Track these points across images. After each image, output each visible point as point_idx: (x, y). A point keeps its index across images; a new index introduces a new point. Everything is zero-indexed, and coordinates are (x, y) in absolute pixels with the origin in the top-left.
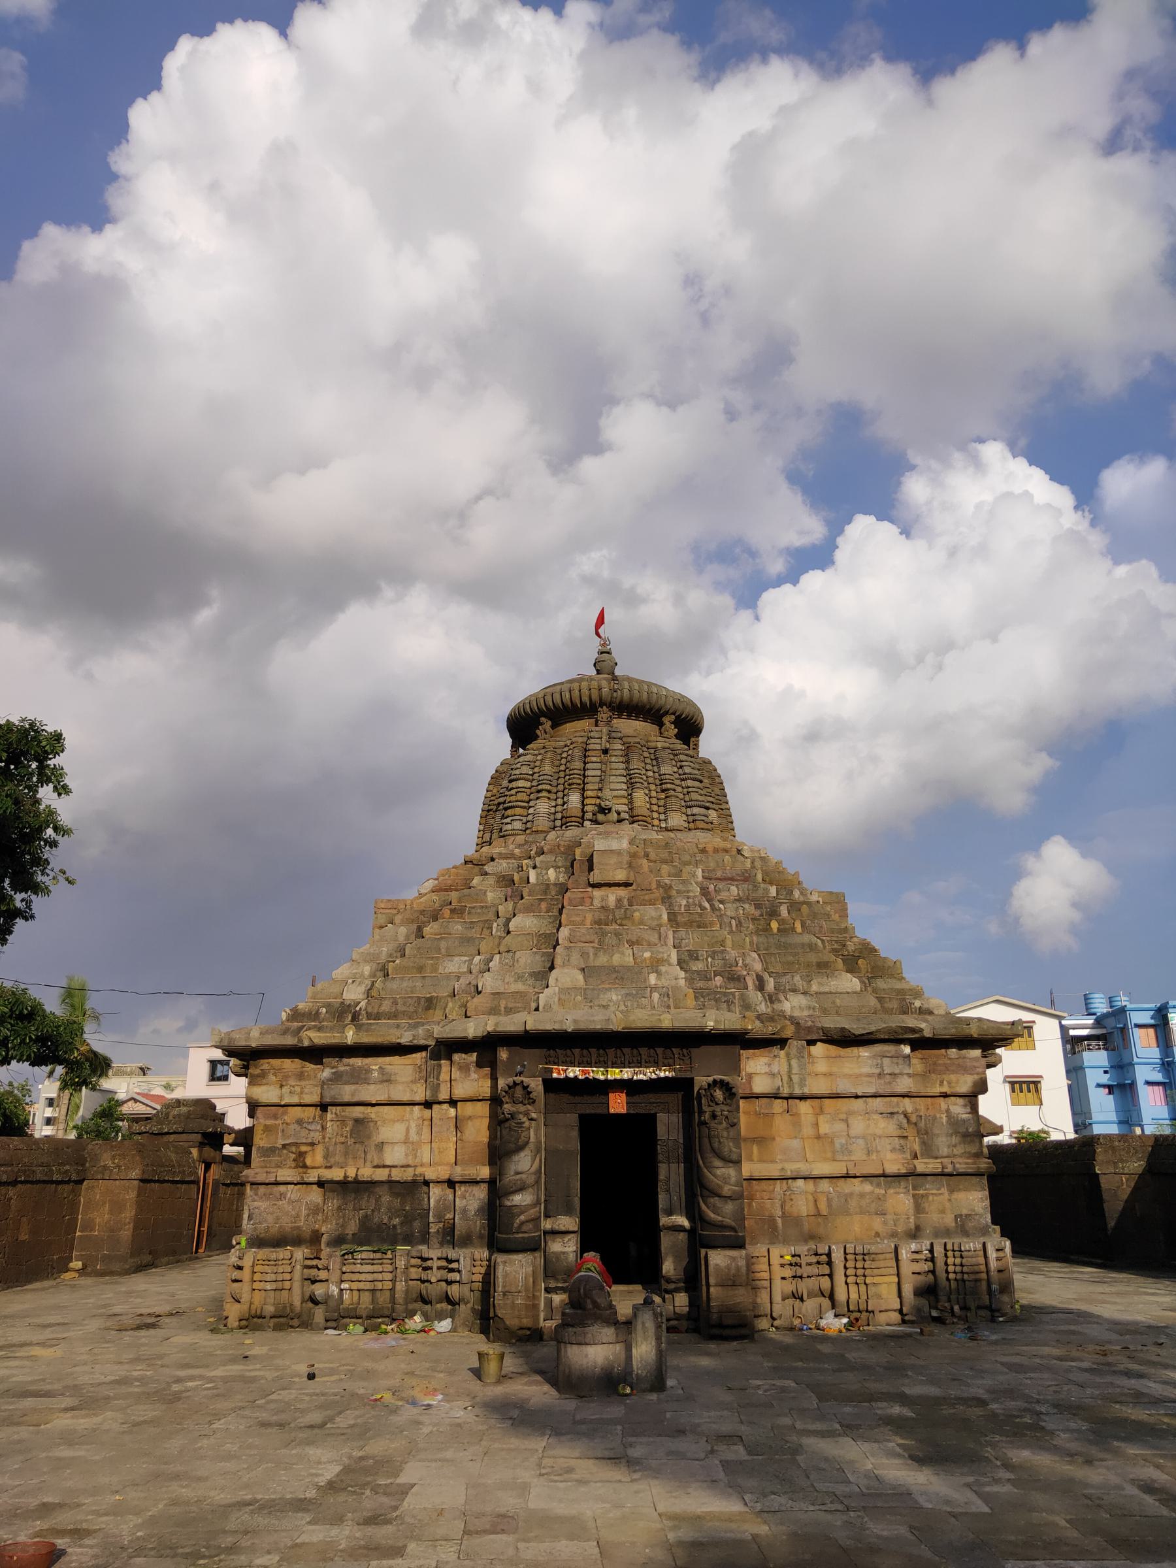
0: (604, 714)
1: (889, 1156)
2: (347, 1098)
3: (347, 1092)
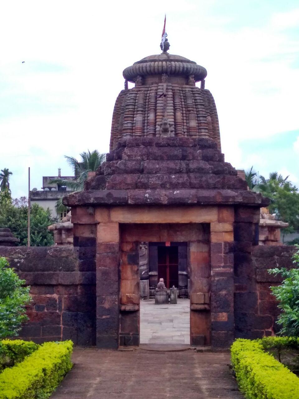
0: (164, 77)
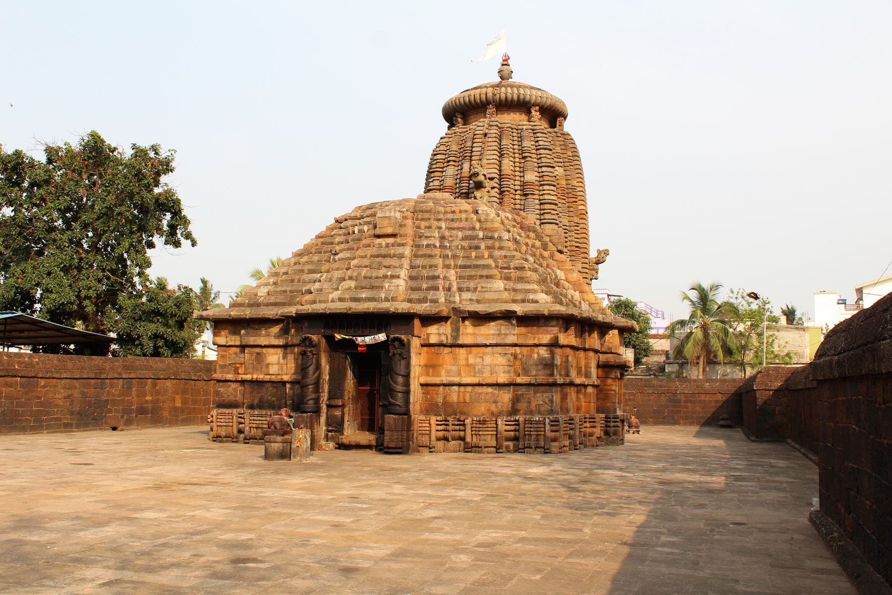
0: (491, 109)
1: (502, 375)
2: (252, 343)
3: (252, 340)
